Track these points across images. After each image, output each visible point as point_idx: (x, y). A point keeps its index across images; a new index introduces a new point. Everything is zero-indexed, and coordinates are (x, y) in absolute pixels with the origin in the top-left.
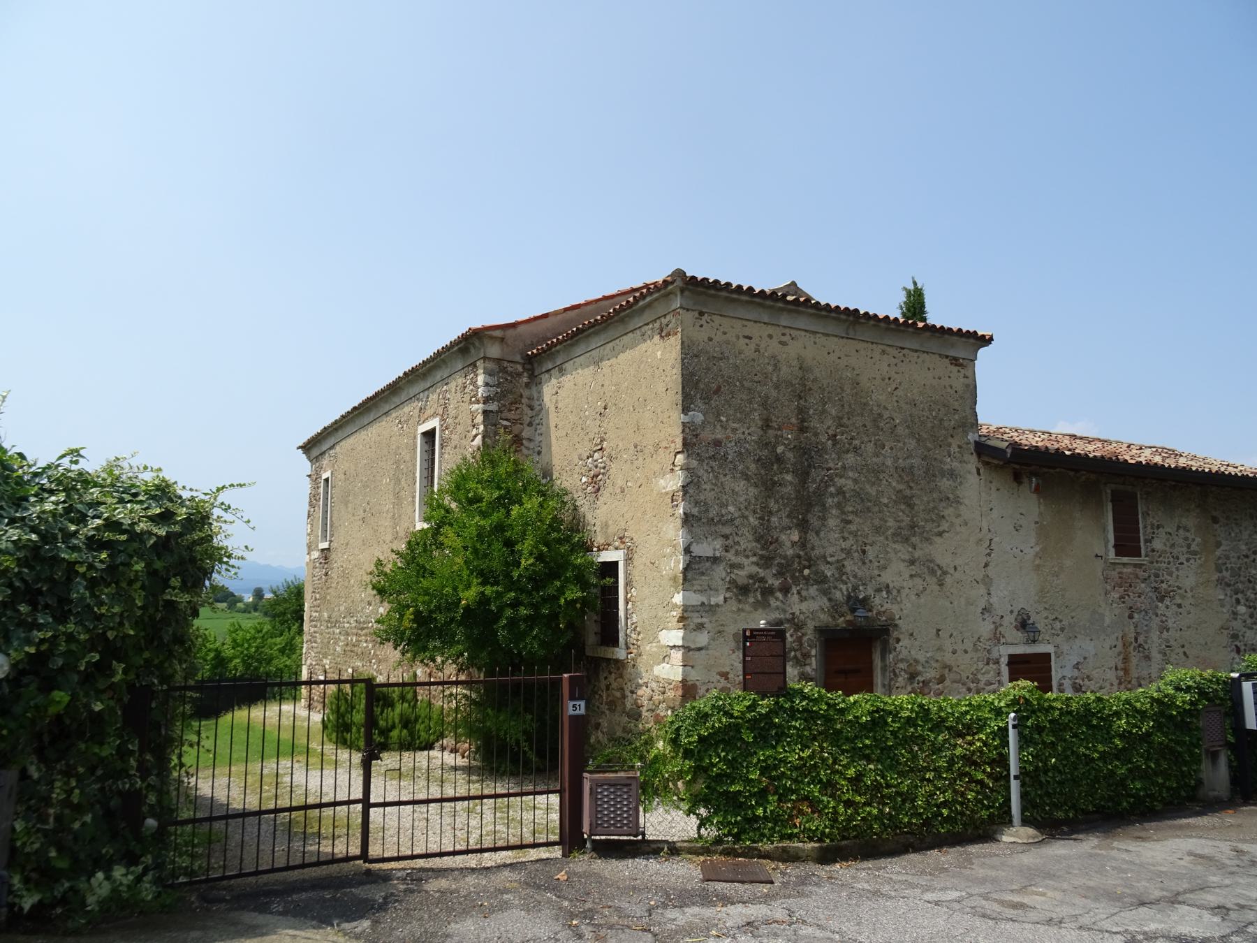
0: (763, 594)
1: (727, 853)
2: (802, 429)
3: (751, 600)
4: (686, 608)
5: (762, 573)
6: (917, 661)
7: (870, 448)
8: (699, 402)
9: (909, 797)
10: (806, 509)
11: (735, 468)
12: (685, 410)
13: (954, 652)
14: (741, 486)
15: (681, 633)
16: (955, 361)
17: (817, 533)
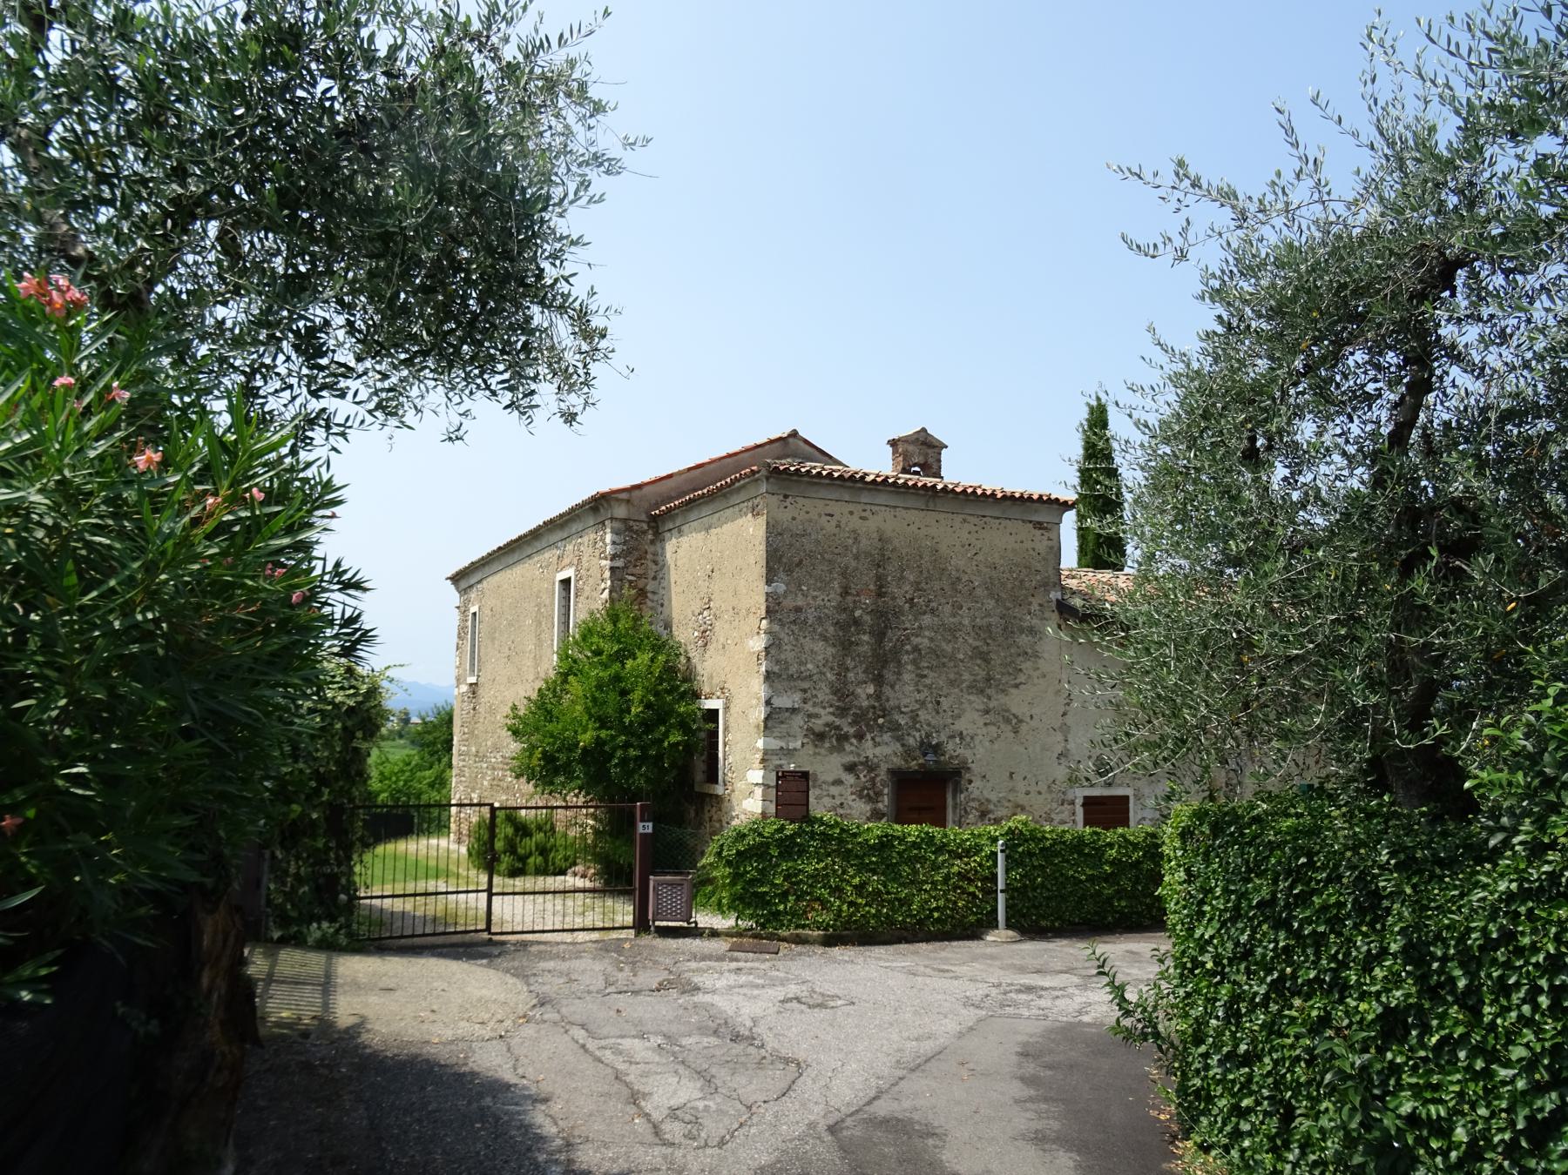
0: (838, 740)
1: (755, 936)
2: (880, 595)
3: (827, 745)
4: (766, 752)
5: (838, 722)
6: (988, 801)
7: (948, 609)
8: (782, 575)
9: (906, 902)
10: (881, 666)
11: (815, 630)
12: (769, 582)
13: (1028, 793)
14: (819, 646)
15: (762, 773)
16: (1039, 526)
17: (892, 687)
